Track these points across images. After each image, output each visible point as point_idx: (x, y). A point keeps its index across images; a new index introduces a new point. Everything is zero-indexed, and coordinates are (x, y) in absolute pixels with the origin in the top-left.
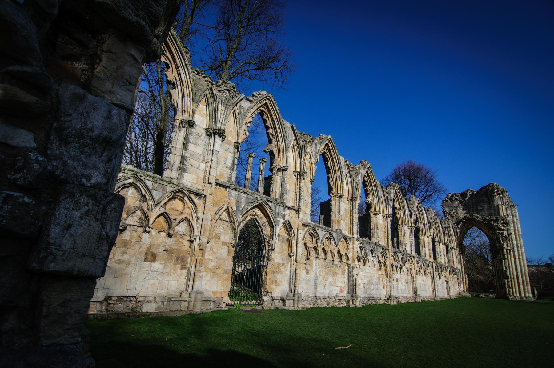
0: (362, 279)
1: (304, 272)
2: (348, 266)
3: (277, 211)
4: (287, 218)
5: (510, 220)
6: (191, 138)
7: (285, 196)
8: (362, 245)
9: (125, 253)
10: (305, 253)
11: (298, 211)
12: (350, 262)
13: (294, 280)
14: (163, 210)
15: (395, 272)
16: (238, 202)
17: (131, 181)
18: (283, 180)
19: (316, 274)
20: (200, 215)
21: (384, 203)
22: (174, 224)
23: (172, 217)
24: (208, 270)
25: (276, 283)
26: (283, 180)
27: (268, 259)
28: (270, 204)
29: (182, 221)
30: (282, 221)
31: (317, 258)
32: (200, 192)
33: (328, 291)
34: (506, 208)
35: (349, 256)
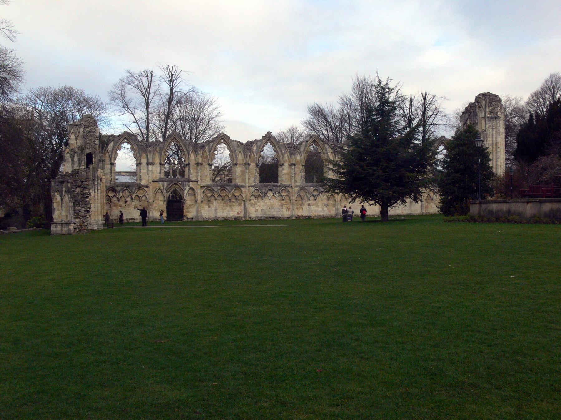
0: (260, 206)
1: (207, 207)
2: (244, 201)
3: (184, 184)
4: (191, 186)
5: (489, 133)
6: (142, 168)
7: (190, 176)
8: (257, 188)
9: (129, 208)
10: (206, 198)
11: (197, 182)
12: (244, 199)
13: (197, 211)
14: (136, 194)
15: (306, 200)
16: (163, 186)
17: (125, 188)
18: (189, 169)
19: (216, 207)
20: (148, 193)
21: (289, 157)
22: (141, 198)
23: (139, 196)
24: (155, 209)
25: (189, 212)
26: (189, 169)
27: (184, 203)
28: (180, 182)
29: (143, 196)
30: (188, 187)
31: (216, 200)
32: (148, 186)
33: (226, 214)
34: (485, 121)
35: (244, 196)
